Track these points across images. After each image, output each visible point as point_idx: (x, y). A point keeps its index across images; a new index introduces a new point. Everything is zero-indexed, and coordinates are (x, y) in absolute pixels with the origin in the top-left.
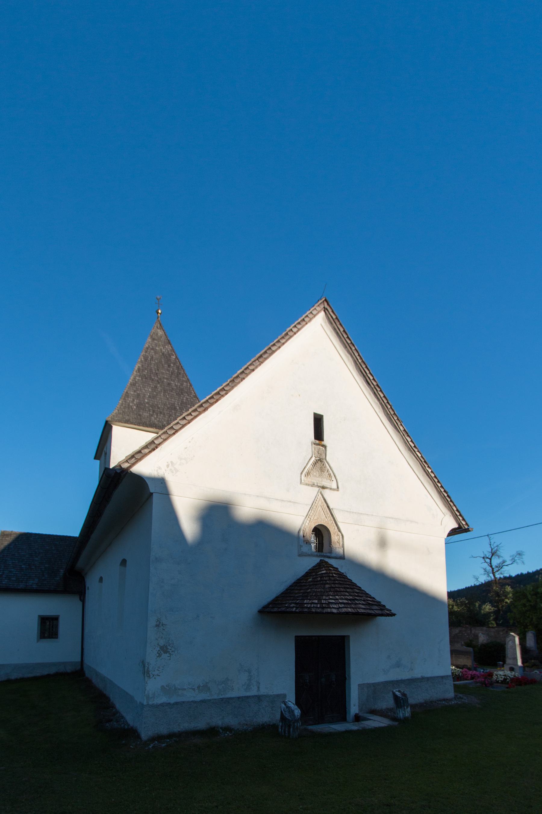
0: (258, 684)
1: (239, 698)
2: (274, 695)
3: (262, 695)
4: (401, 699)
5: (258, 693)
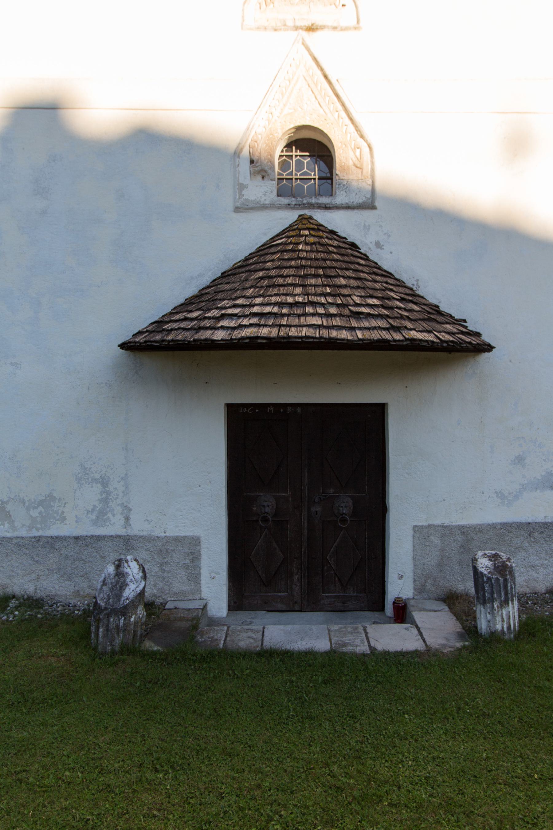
0: (125, 511)
1: (77, 538)
2: (165, 536)
3: (136, 536)
4: (485, 579)
5: (125, 530)
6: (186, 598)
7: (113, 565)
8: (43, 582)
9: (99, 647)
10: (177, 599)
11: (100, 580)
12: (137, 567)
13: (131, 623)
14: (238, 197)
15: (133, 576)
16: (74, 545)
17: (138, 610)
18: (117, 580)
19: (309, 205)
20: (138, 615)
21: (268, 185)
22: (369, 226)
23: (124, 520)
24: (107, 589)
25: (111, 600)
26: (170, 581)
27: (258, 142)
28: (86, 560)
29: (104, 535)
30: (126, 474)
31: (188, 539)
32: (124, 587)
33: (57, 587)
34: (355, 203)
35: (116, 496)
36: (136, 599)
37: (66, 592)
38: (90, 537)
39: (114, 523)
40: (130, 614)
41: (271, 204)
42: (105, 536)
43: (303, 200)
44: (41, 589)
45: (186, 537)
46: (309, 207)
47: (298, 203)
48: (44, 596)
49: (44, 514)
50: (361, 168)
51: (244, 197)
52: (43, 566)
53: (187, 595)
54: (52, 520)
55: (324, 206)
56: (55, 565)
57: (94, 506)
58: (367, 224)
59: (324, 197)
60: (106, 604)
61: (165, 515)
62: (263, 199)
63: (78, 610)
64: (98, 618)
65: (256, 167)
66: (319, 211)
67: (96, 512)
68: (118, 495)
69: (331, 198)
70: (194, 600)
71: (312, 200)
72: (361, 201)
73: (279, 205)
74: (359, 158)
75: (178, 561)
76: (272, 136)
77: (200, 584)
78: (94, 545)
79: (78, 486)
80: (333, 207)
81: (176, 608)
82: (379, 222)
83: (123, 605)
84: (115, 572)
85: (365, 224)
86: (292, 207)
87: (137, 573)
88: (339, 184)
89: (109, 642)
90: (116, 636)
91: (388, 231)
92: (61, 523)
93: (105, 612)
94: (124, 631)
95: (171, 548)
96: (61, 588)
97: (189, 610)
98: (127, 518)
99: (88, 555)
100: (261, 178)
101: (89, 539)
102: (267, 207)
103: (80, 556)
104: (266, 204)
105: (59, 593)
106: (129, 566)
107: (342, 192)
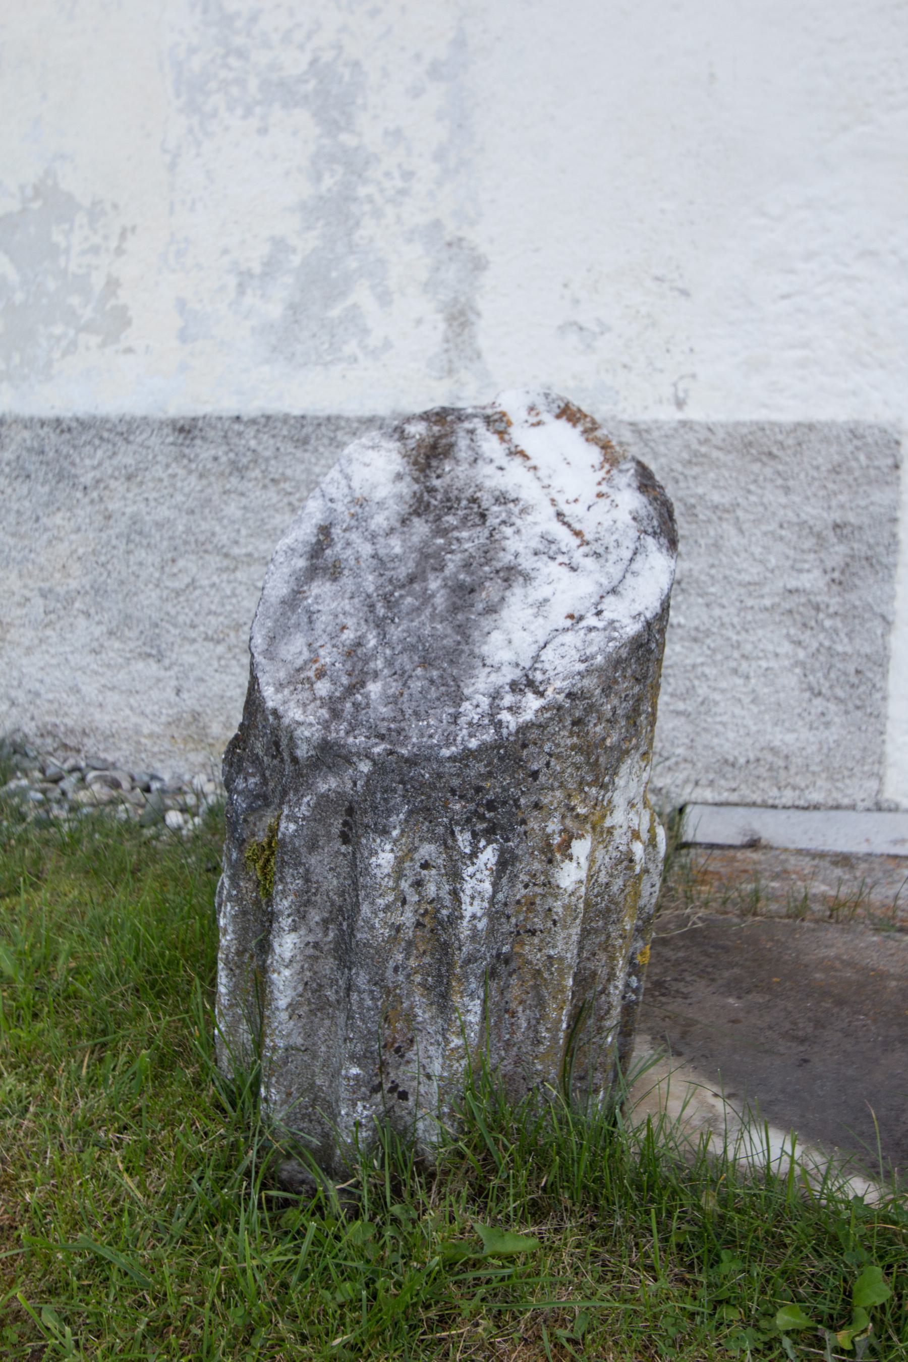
2: (684, 424)
6: (789, 796)
7: (395, 445)
8: (25, 661)
9: (272, 1092)
10: (734, 797)
11: (288, 540)
12: (595, 455)
13: (558, 907)
15: (559, 515)
16: (174, 468)
17: (619, 799)
18: (426, 543)
20: (620, 838)
23: (442, 326)
24: (347, 605)
25: (374, 688)
26: (702, 690)
28: (236, 551)
29: (333, 411)
30: (460, 43)
31: (825, 440)
32: (492, 590)
33: (90, 690)
35: (399, 183)
36: (607, 690)
37: (134, 719)
38: (253, 421)
39: (387, 345)
40: (553, 826)
42: (338, 417)
44: (13, 693)
45: (811, 427)
48: (30, 728)
49: (19, 297)
52: (20, 576)
53: (800, 781)
54: (58, 330)
56: (75, 568)
57: (279, 245)
60: (336, 714)
61: (685, 293)
63: (184, 810)
64: (262, 837)
67: (289, 280)
68: (408, 175)
70: (838, 807)
75: (754, 572)
77: (878, 716)
78: (275, 470)
79: (190, 130)
81: (753, 844)
83: (489, 736)
84: (406, 488)
87: (589, 493)
89: (354, 1058)
90: (422, 1015)
92: (103, 345)
93: (327, 784)
94: (492, 974)
95: (716, 497)
96: (113, 698)
97: (844, 860)
98: (462, 313)
99: (245, 520)
101: (251, 431)
103: (204, 526)
105: (103, 719)
106: (518, 453)
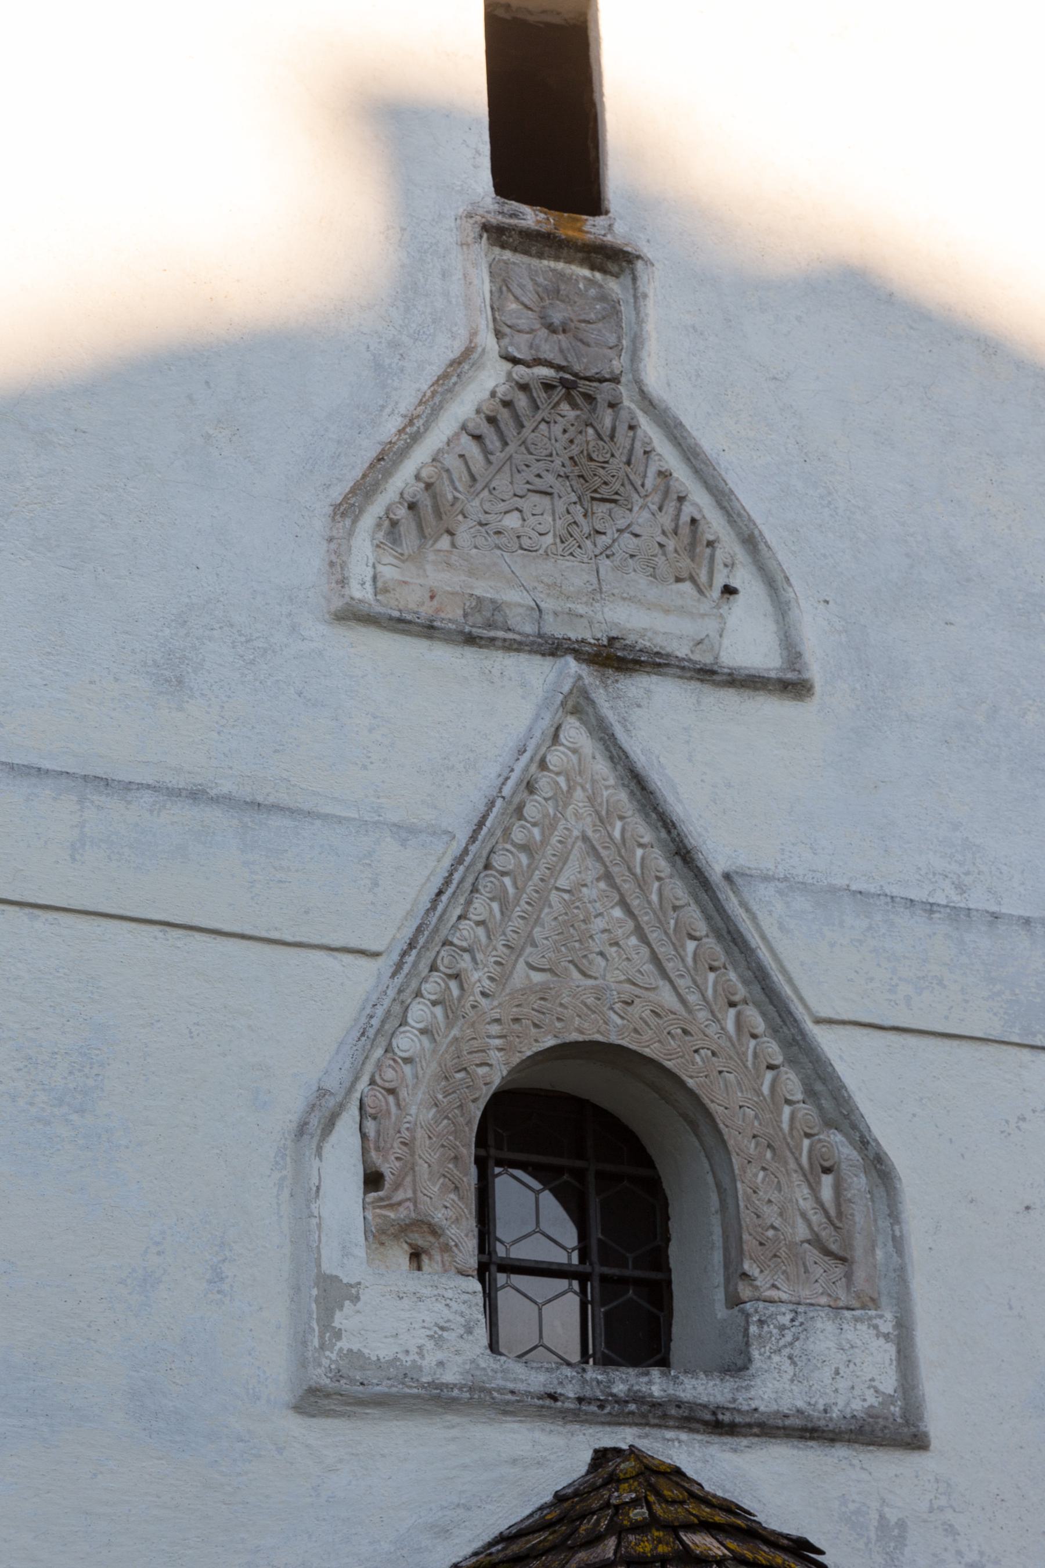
14: (316, 1343)
19: (645, 1408)
21: (449, 1294)
22: (902, 1525)
27: (403, 1093)
34: (835, 1414)
41: (471, 1389)
43: (611, 1382)
46: (644, 1416)
47: (588, 1393)
50: (843, 1260)
51: (343, 1344)
55: (708, 1417)
58: (892, 1516)
59: (702, 1375)
62: (430, 1361)
65: (391, 1206)
66: (684, 1436)
69: (730, 1384)
71: (650, 1383)
72: (857, 1406)
73: (509, 1397)
74: (833, 1212)
76: (459, 1076)
80: (749, 1425)
82: (941, 1509)
85: (882, 1516)
86: (568, 1410)
88: (761, 1323)
91: (981, 1553)
100: (404, 1261)
102: (455, 1400)
104: (451, 1387)
107: (776, 1358)
